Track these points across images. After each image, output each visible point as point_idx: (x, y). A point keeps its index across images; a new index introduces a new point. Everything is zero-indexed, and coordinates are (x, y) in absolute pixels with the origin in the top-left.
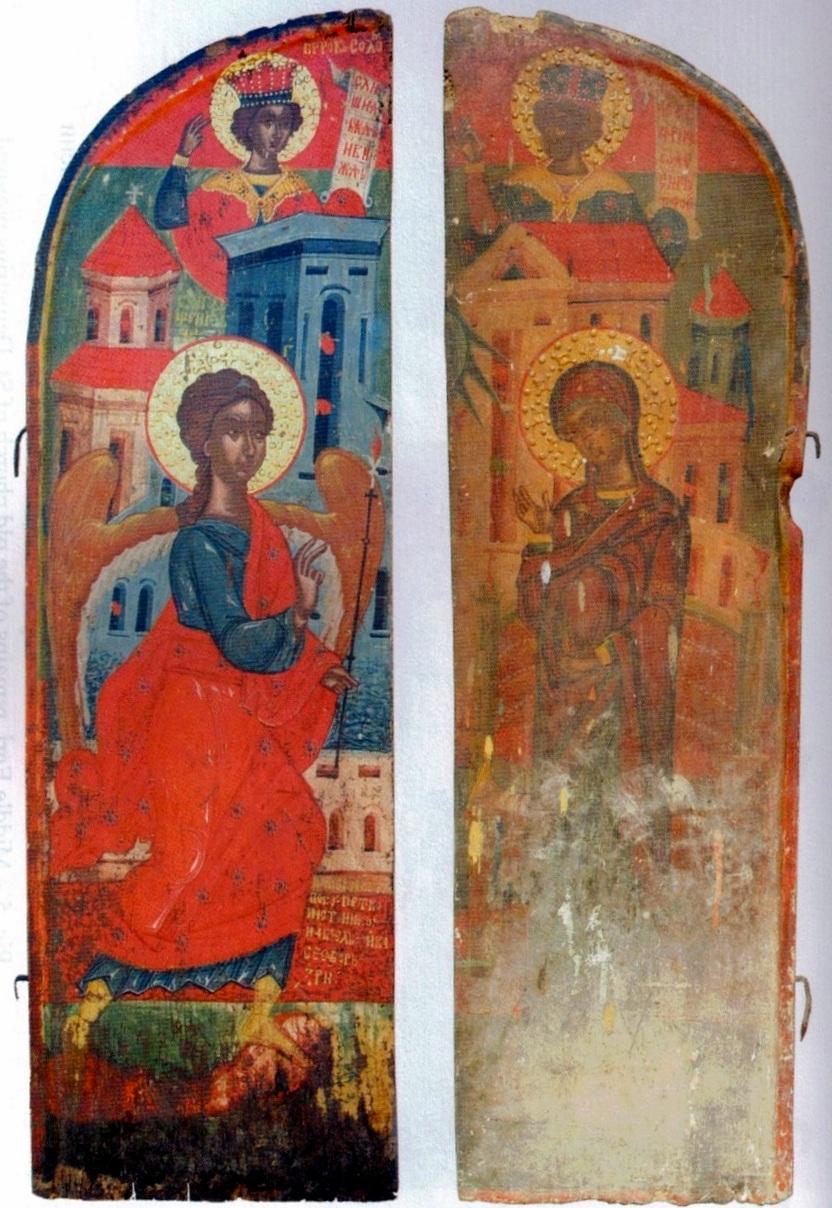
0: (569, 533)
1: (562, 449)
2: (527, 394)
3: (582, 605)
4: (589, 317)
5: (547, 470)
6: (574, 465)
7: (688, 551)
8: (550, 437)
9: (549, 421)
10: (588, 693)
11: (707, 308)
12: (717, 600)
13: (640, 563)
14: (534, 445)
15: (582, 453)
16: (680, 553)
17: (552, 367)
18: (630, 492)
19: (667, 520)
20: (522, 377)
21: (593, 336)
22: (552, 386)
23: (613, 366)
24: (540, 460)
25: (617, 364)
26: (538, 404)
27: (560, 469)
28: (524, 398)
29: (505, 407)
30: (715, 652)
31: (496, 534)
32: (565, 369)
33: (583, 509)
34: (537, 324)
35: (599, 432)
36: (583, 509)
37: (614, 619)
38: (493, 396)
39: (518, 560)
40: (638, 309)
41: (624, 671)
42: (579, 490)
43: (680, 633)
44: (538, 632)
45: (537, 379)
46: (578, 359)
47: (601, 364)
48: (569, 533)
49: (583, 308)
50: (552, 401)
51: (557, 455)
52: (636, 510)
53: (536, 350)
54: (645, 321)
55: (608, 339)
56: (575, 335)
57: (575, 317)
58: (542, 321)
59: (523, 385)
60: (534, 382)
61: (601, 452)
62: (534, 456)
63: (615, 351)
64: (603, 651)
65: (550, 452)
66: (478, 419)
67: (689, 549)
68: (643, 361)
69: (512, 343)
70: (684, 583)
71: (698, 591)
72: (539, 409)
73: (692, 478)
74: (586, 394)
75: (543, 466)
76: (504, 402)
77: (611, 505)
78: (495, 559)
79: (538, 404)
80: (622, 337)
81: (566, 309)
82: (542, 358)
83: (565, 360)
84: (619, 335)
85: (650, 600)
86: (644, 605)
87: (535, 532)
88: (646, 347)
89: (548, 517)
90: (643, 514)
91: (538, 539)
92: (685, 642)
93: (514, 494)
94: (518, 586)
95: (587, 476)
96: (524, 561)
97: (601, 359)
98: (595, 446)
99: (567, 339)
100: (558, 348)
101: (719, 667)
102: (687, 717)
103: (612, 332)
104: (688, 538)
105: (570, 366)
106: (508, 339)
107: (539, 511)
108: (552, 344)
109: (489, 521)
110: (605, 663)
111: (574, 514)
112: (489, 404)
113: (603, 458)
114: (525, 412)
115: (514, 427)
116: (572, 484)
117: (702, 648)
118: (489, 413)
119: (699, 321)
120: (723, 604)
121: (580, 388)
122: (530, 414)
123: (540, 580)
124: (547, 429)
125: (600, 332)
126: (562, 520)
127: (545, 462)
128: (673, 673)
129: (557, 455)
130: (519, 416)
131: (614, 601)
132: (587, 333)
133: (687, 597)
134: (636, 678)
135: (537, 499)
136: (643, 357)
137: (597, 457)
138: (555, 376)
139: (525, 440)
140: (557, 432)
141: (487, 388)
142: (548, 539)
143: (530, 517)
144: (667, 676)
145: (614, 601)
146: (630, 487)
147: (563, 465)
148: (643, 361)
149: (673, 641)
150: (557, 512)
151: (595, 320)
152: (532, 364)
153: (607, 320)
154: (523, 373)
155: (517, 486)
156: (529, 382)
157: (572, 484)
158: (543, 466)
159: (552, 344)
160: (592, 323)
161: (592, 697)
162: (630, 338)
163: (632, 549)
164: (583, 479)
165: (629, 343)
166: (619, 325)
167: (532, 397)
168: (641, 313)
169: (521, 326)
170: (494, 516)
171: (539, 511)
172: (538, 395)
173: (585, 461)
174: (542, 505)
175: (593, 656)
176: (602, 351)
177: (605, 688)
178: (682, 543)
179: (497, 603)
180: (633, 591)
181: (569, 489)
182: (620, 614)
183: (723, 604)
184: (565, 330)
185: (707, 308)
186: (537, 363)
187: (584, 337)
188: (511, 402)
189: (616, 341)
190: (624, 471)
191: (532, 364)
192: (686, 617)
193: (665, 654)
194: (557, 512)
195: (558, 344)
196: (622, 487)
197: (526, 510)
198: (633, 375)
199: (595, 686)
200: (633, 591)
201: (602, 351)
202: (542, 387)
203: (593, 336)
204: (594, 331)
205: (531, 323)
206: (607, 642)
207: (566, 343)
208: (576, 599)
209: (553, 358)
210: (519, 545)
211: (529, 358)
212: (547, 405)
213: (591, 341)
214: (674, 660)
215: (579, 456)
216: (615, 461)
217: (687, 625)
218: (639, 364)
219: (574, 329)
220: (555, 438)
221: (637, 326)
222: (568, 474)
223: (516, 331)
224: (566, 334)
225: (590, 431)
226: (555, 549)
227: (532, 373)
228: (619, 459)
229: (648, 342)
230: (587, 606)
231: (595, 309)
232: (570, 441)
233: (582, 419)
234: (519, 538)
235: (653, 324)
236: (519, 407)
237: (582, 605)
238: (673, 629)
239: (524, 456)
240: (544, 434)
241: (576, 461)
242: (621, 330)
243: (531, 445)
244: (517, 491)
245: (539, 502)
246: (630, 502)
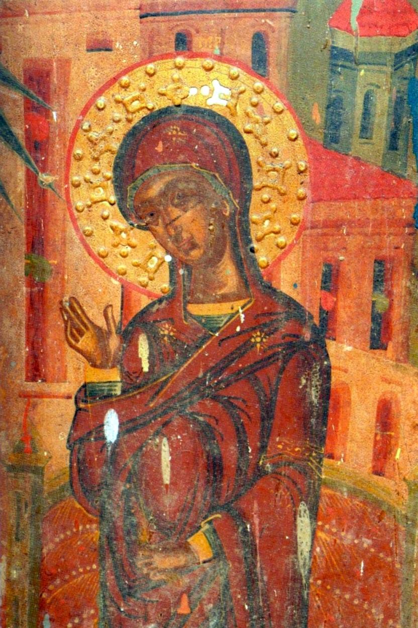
0: (146, 367)
1: (134, 241)
2: (79, 159)
3: (167, 478)
4: (173, 38)
5: (111, 274)
6: (152, 265)
7: (326, 394)
8: (115, 223)
9: (113, 199)
10: (178, 603)
11: (354, 24)
12: (370, 465)
13: (255, 409)
14: (90, 235)
15: (163, 245)
16: (314, 396)
17: (117, 116)
18: (238, 305)
19: (293, 345)
20: (71, 130)
21: (180, 68)
22: (115, 146)
23: (212, 114)
24: (100, 259)
25: (214, 109)
26: (96, 173)
27: (131, 271)
28: (74, 164)
29: (45, 178)
30: (367, 542)
31: (35, 370)
32: (137, 118)
33: (166, 330)
34: (90, 49)
35: (189, 214)
36: (166, 330)
37: (217, 493)
38: (27, 161)
39: (70, 407)
40: (248, 25)
41: (225, 569)
42: (160, 301)
43: (315, 514)
44: (102, 514)
45: (93, 135)
46: (156, 103)
47: (194, 110)
48: (146, 367)
49: (162, 25)
50: (117, 167)
51: (126, 250)
52: (248, 331)
53: (93, 87)
54: (259, 42)
55: (203, 73)
56: (150, 67)
57: (151, 38)
58: (100, 46)
59: (73, 139)
60: (90, 140)
61: (194, 246)
62: (90, 253)
63: (212, 91)
64: (200, 544)
65: (115, 246)
66: (7, 198)
67: (329, 389)
68: (255, 105)
69: (55, 80)
70: (322, 440)
71: (338, 451)
72: (96, 180)
73: (36, 305)
74: (170, 156)
75: (104, 268)
76: (43, 170)
77: (209, 323)
78: (35, 406)
79: (96, 173)
80: (223, 69)
81: (137, 25)
82: (101, 102)
83: (136, 105)
84: (217, 65)
85: (269, 467)
86: (260, 472)
87: (94, 365)
88: (259, 84)
89: (114, 343)
90: (257, 338)
91: (96, 376)
92: (322, 528)
93: (62, 309)
94: (70, 447)
95: (172, 281)
96: (78, 410)
97: (190, 102)
98: (185, 235)
99: (139, 73)
100: (126, 87)
101: (373, 565)
102: (126, 458)
103: (208, 62)
104: (326, 373)
105: (143, 114)
106: (48, 74)
107: (101, 336)
108: (115, 79)
109: (25, 350)
110: (202, 558)
111: (154, 339)
112: (21, 175)
113: (195, 254)
114: (77, 186)
115: (59, 210)
116: (150, 295)
117: (348, 538)
118: (21, 187)
119: (342, 41)
120: (378, 471)
121: (160, 148)
122: (84, 186)
123: (104, 438)
124: (107, 210)
125: (190, 63)
126: (136, 347)
127: (107, 261)
128: (304, 572)
129: (126, 250)
130: (67, 190)
131: (215, 467)
132: (169, 63)
133: (326, 461)
134: (250, 580)
135: (96, 316)
136: (255, 100)
137: (187, 253)
138: (122, 130)
139: (77, 229)
140: (126, 216)
141: (19, 150)
142: (114, 375)
143: (86, 342)
144: (296, 578)
145: (215, 467)
146: (239, 298)
147: (137, 265)
148: (255, 105)
149: (304, 525)
150: (128, 337)
151: (183, 42)
152: (84, 112)
153: (198, 43)
154: (71, 125)
155: (67, 298)
156: (81, 138)
157: (150, 295)
158: (104, 268)
159: (115, 79)
160: (177, 47)
161: (184, 609)
162: (235, 70)
163: (239, 391)
164: (166, 285)
165: (234, 78)
166: (217, 52)
167: (86, 162)
168: (252, 31)
169: (68, 52)
170: (33, 344)
171: (101, 336)
172: (96, 159)
173: (168, 258)
174: (105, 327)
175: (185, 547)
176: (193, 92)
177: (204, 595)
178: (316, 381)
179: (39, 472)
180: (243, 452)
181: (145, 301)
182: (224, 485)
183: (378, 471)
184: (137, 58)
185: (354, 24)
186: (93, 109)
187: (164, 69)
188: (52, 172)
189: (212, 75)
190: (228, 272)
191: (84, 112)
192: (325, 491)
193: (292, 547)
194: (128, 337)
195: (125, 79)
196: (225, 298)
197: (81, 334)
198: (239, 127)
199: (188, 591)
200: (243, 452)
201: (193, 92)
202: (102, 146)
203: (180, 68)
204: (180, 60)
205: (83, 47)
206: (205, 527)
207: (138, 78)
208: (159, 472)
209: (118, 102)
210: (71, 387)
211: (80, 103)
212: (109, 174)
213: (176, 74)
214: (306, 554)
215: (160, 252)
216: (213, 261)
217: (322, 505)
218: (250, 109)
219: (151, 59)
220: (122, 224)
221: (245, 52)
222: (144, 279)
223: (59, 60)
224: (138, 65)
225: (176, 212)
226: (124, 392)
227: (86, 126)
228: (220, 254)
229: (262, 77)
230: (173, 475)
231: (181, 24)
232: (146, 228)
233: (163, 194)
234: (71, 375)
235: (272, 50)
236: (67, 178)
237: (167, 478)
238: (303, 507)
239: (76, 252)
240: (105, 219)
241: (155, 259)
242: (220, 58)
243: (85, 236)
244: (67, 305)
245: (101, 322)
246: (238, 322)
